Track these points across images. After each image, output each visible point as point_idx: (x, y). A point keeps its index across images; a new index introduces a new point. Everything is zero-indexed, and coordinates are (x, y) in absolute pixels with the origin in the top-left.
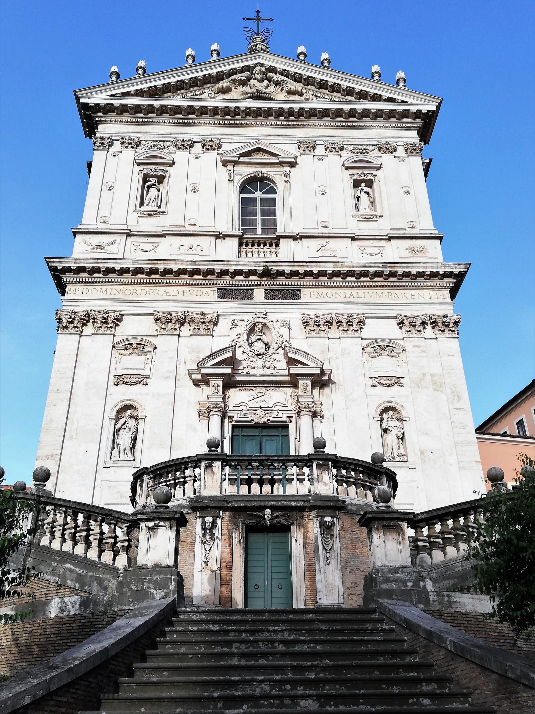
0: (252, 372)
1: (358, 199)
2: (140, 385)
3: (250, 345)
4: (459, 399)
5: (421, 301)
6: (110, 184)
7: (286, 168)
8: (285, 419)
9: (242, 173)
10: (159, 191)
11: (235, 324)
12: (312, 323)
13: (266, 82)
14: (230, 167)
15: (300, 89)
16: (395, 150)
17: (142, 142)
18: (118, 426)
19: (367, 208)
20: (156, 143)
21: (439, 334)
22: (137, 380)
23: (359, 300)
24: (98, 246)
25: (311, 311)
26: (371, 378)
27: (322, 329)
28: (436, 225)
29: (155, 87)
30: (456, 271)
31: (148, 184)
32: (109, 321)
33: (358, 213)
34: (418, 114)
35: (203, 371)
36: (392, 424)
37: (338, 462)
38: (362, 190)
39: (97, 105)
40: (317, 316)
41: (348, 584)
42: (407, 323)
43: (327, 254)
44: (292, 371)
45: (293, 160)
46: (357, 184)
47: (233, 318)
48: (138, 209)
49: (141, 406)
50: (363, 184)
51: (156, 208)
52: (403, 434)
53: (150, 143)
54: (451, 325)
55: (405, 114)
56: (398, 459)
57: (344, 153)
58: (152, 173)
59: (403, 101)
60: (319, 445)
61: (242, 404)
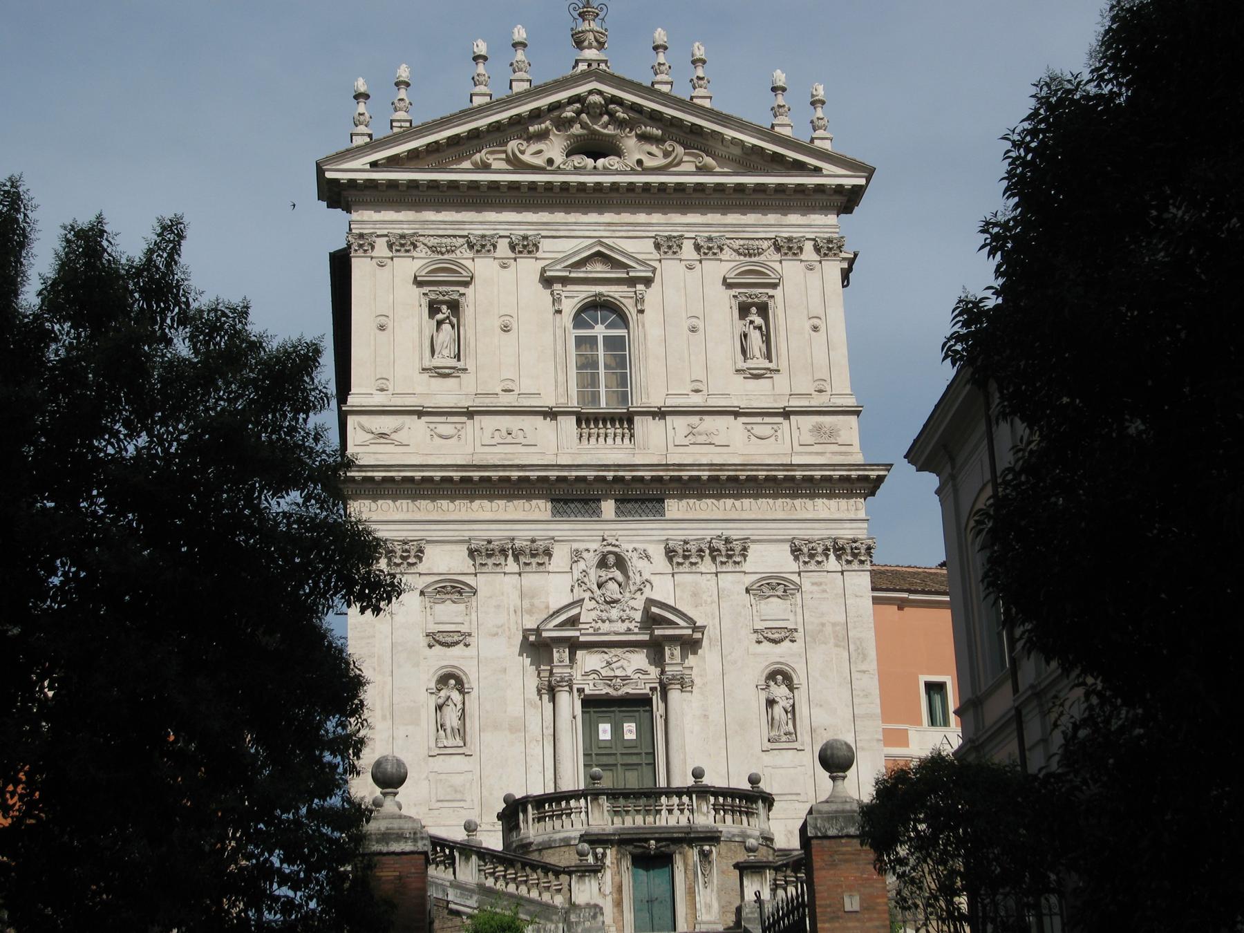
0: (605, 627)
1: (745, 336)
2: (461, 645)
3: (600, 586)
4: (865, 657)
5: (824, 514)
6: (383, 320)
7: (640, 287)
8: (647, 691)
9: (575, 294)
10: (453, 327)
11: (577, 556)
12: (680, 551)
13: (606, 118)
14: (557, 287)
15: (658, 132)
16: (801, 249)
17: (421, 239)
18: (441, 701)
19: (758, 355)
20: (444, 240)
21: (846, 567)
22: (456, 638)
23: (745, 516)
24: (382, 435)
25: (677, 534)
26: (756, 631)
27: (693, 560)
28: (855, 391)
29: (436, 142)
30: (873, 474)
31: (440, 316)
32: (413, 553)
33: (745, 366)
34: (839, 189)
35: (545, 634)
36: (780, 691)
37: (717, 792)
38: (751, 322)
39: (352, 182)
40: (686, 542)
41: (723, 903)
42: (805, 550)
43: (701, 439)
44: (657, 632)
45: (650, 274)
46: (744, 310)
47: (575, 546)
48: (427, 364)
49: (465, 674)
50: (754, 310)
51: (453, 363)
52: (793, 706)
53: (433, 241)
54: (863, 551)
55: (820, 189)
56: (784, 738)
57: (727, 254)
58: (441, 298)
59: (817, 171)
60: (698, 774)
61: (595, 672)
